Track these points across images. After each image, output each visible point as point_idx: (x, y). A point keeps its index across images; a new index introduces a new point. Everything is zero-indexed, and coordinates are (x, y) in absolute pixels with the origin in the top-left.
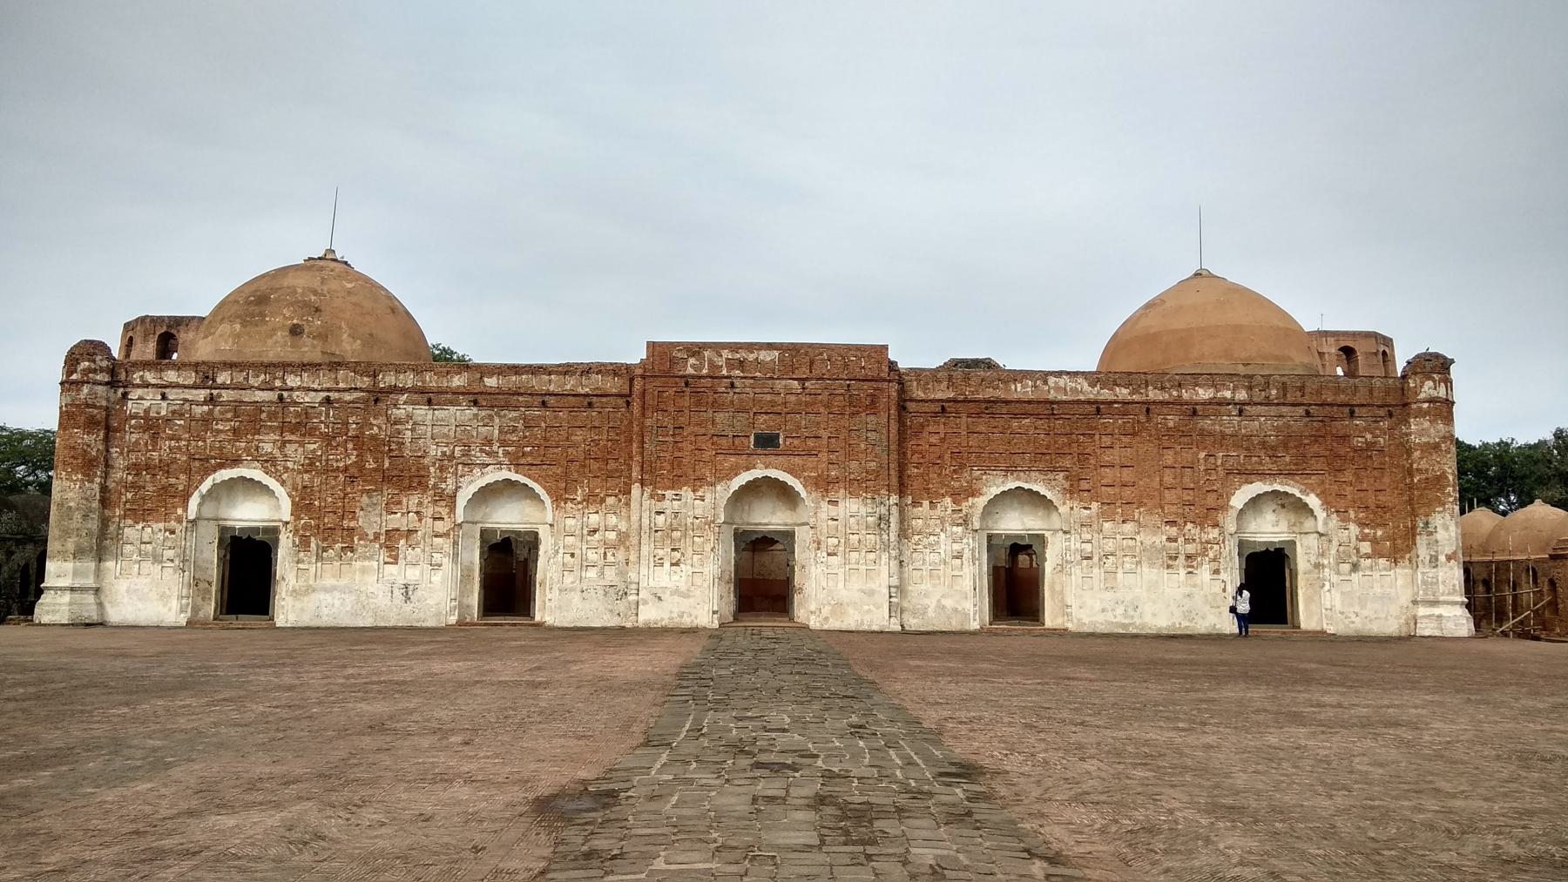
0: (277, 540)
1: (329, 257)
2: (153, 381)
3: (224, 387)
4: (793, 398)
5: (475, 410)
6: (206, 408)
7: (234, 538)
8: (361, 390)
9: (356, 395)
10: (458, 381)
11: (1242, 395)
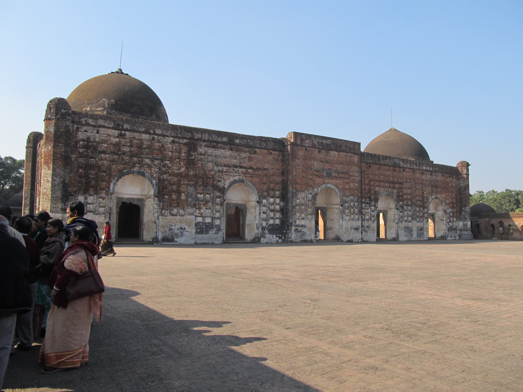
0: (144, 205)
1: (120, 72)
2: (92, 124)
3: (127, 130)
5: (230, 151)
6: (117, 140)
7: (123, 203)
8: (186, 138)
9: (185, 141)
10: (225, 139)
11: (431, 169)
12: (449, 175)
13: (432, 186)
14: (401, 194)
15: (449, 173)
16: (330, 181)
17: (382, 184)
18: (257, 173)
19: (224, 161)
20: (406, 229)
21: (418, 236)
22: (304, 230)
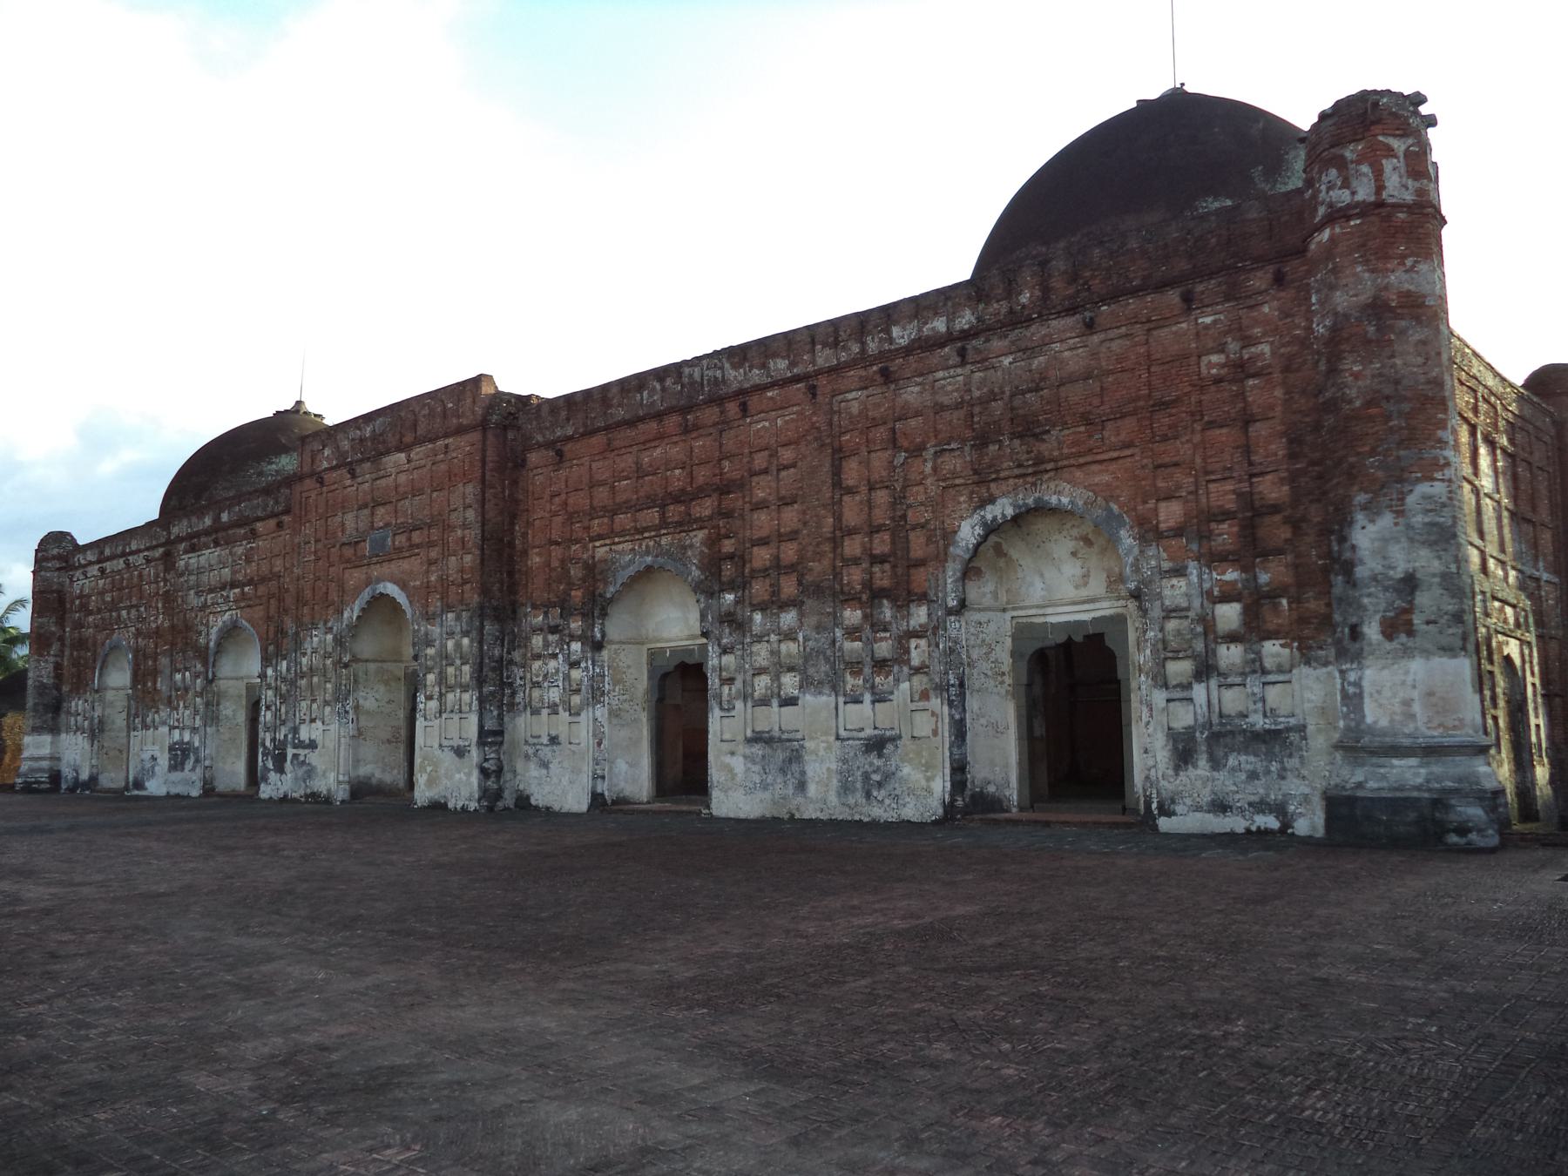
4: (402, 478)
12: (1173, 297)
13: (982, 441)
14: (728, 546)
15: (1162, 286)
16: (386, 569)
17: (623, 519)
18: (262, 590)
19: (213, 578)
20: (758, 750)
21: (845, 788)
22: (314, 758)
